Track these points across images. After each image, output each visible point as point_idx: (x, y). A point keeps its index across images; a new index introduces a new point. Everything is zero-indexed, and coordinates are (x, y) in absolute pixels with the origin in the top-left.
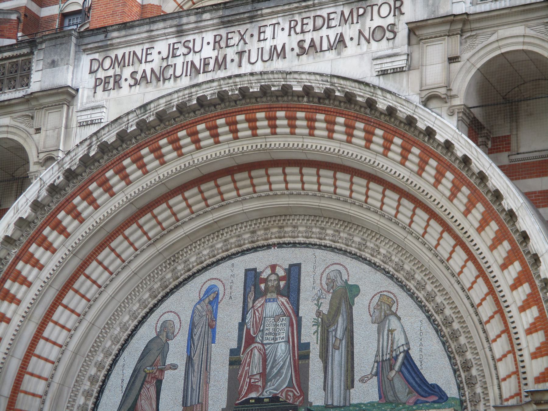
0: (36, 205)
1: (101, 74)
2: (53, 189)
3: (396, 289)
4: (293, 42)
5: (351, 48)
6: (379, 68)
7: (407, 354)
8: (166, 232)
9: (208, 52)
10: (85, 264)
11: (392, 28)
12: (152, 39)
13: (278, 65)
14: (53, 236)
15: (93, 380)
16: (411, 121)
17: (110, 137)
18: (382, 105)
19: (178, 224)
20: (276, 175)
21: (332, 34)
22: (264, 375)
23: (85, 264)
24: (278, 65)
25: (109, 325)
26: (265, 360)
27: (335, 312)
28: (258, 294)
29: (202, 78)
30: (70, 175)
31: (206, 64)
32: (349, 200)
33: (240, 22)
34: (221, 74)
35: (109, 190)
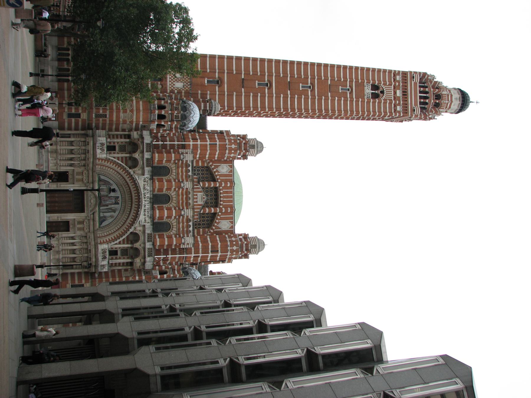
0: (128, 171)
1: (146, 179)
2: (130, 173)
3: (115, 218)
5: (144, 217)
6: (141, 221)
7: (106, 220)
8: (125, 186)
9: (147, 196)
10: (121, 175)
11: (146, 222)
13: (143, 206)
15: (105, 174)
16: (133, 226)
17: (136, 182)
18: (135, 221)
19: (126, 188)
20: (130, 203)
21: (146, 214)
22: (104, 200)
23: (121, 175)
25: (113, 176)
26: (107, 200)
29: (143, 195)
30: (132, 175)
31: (145, 196)
33: (150, 200)
34: (143, 198)
35: (130, 180)
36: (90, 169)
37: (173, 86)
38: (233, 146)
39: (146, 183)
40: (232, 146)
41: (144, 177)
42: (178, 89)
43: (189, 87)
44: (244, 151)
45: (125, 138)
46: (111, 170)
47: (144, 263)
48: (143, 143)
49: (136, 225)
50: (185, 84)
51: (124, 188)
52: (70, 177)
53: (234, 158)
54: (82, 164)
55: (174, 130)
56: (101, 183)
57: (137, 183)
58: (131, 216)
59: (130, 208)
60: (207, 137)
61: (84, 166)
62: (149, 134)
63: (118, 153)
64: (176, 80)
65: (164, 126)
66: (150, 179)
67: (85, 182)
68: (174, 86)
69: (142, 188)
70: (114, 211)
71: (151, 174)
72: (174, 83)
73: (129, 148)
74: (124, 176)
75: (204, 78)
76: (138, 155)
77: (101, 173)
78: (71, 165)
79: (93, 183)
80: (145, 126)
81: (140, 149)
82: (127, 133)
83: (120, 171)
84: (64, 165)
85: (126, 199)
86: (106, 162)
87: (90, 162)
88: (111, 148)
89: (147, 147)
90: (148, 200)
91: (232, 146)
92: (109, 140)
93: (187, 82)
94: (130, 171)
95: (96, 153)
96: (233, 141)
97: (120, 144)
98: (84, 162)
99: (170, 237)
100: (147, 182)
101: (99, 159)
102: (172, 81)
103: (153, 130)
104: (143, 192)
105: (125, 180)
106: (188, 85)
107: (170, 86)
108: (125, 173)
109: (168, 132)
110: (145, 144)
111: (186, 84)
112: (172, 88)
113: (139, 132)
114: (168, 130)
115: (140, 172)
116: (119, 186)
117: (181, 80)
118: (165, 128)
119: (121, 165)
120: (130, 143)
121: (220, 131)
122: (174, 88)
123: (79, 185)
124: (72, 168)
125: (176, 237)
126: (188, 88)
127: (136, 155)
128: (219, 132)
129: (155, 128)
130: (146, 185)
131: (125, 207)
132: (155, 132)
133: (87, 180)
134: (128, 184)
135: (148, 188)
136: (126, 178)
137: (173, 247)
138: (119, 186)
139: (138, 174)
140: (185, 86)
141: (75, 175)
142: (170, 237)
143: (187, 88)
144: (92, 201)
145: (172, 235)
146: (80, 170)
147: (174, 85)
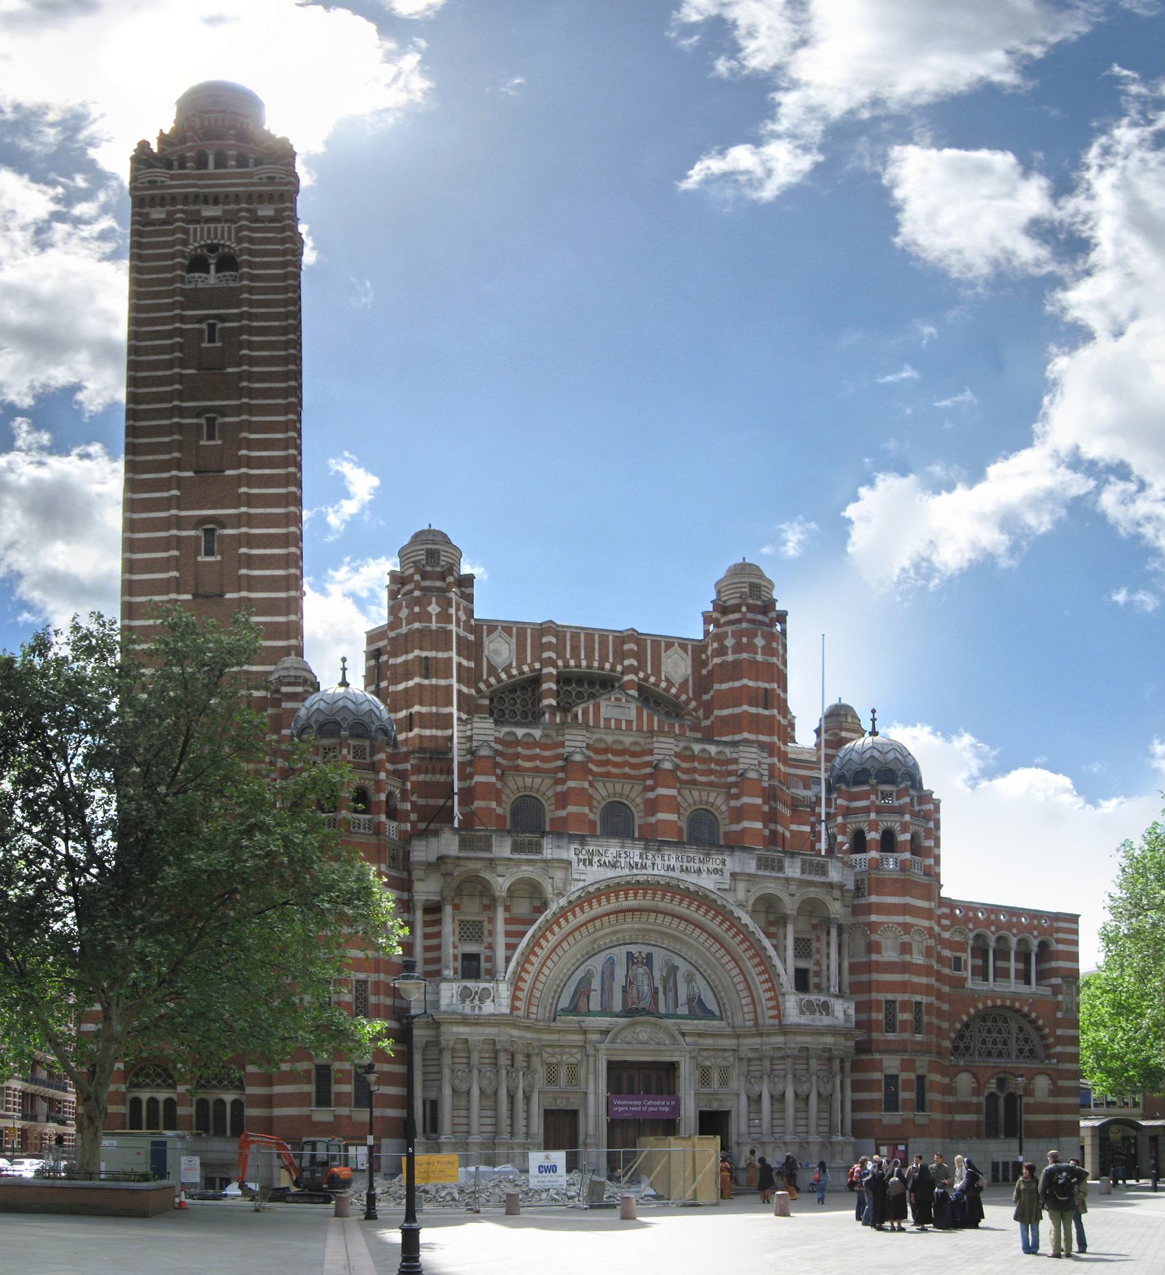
2: (563, 908)
4: (678, 865)
8: (596, 930)
9: (637, 859)
12: (608, 846)
13: (671, 874)
14: (556, 929)
17: (591, 889)
20: (653, 915)
22: (639, 999)
24: (671, 874)
27: (669, 975)
28: (634, 964)
29: (635, 871)
30: (570, 902)
32: (683, 932)
34: (644, 871)
36: (539, 1040)
38: (434, 609)
39: (596, 859)
40: (434, 613)
41: (575, 864)
44: (450, 579)
45: (438, 922)
46: (545, 970)
47: (841, 887)
48: (459, 858)
49: (729, 897)
51: (602, 933)
52: (561, 1104)
53: (470, 613)
54: (525, 1064)
55: (400, 767)
56: (583, 1008)
57: (596, 886)
58: (699, 916)
59: (668, 919)
60: (401, 687)
61: (528, 1056)
62: (424, 843)
63: (490, 947)
65: (390, 795)
66: (583, 844)
67: (578, 1056)
69: (610, 873)
70: (673, 970)
71: (564, 842)
73: (472, 909)
74: (567, 927)
76: (500, 880)
77: (551, 1004)
78: (527, 1098)
79: (585, 1032)
80: (393, 858)
81: (479, 871)
82: (419, 915)
83: (553, 940)
84: (524, 1122)
85: (638, 930)
86: (521, 984)
87: (520, 1037)
88: (471, 967)
89: (472, 848)
90: (650, 857)
91: (434, 613)
92: (448, 973)
94: (554, 907)
95: (493, 1015)
96: (417, 609)
97: (457, 938)
98: (520, 1059)
99: (738, 814)
100: (592, 854)
101: (513, 1008)
103: (402, 833)
104: (626, 871)
105: (578, 928)
108: (560, 927)
109: (409, 786)
110: (463, 854)
113: (417, 874)
114: (404, 784)
115: (559, 874)
116: (593, 949)
118: (397, 792)
119: (533, 936)
120: (456, 907)
121: (367, 659)
123: (591, 1077)
124: (535, 1096)
125: (737, 797)
127: (501, 884)
128: (373, 662)
129: (395, 824)
130: (603, 859)
131: (661, 933)
132: (408, 827)
133: (574, 1051)
134: (592, 920)
135: (612, 852)
136: (574, 922)
137: (766, 808)
138: (593, 949)
139: (566, 882)
141: (556, 1088)
142: (738, 814)
144: (644, 1036)
145: (731, 809)
146: (541, 1073)
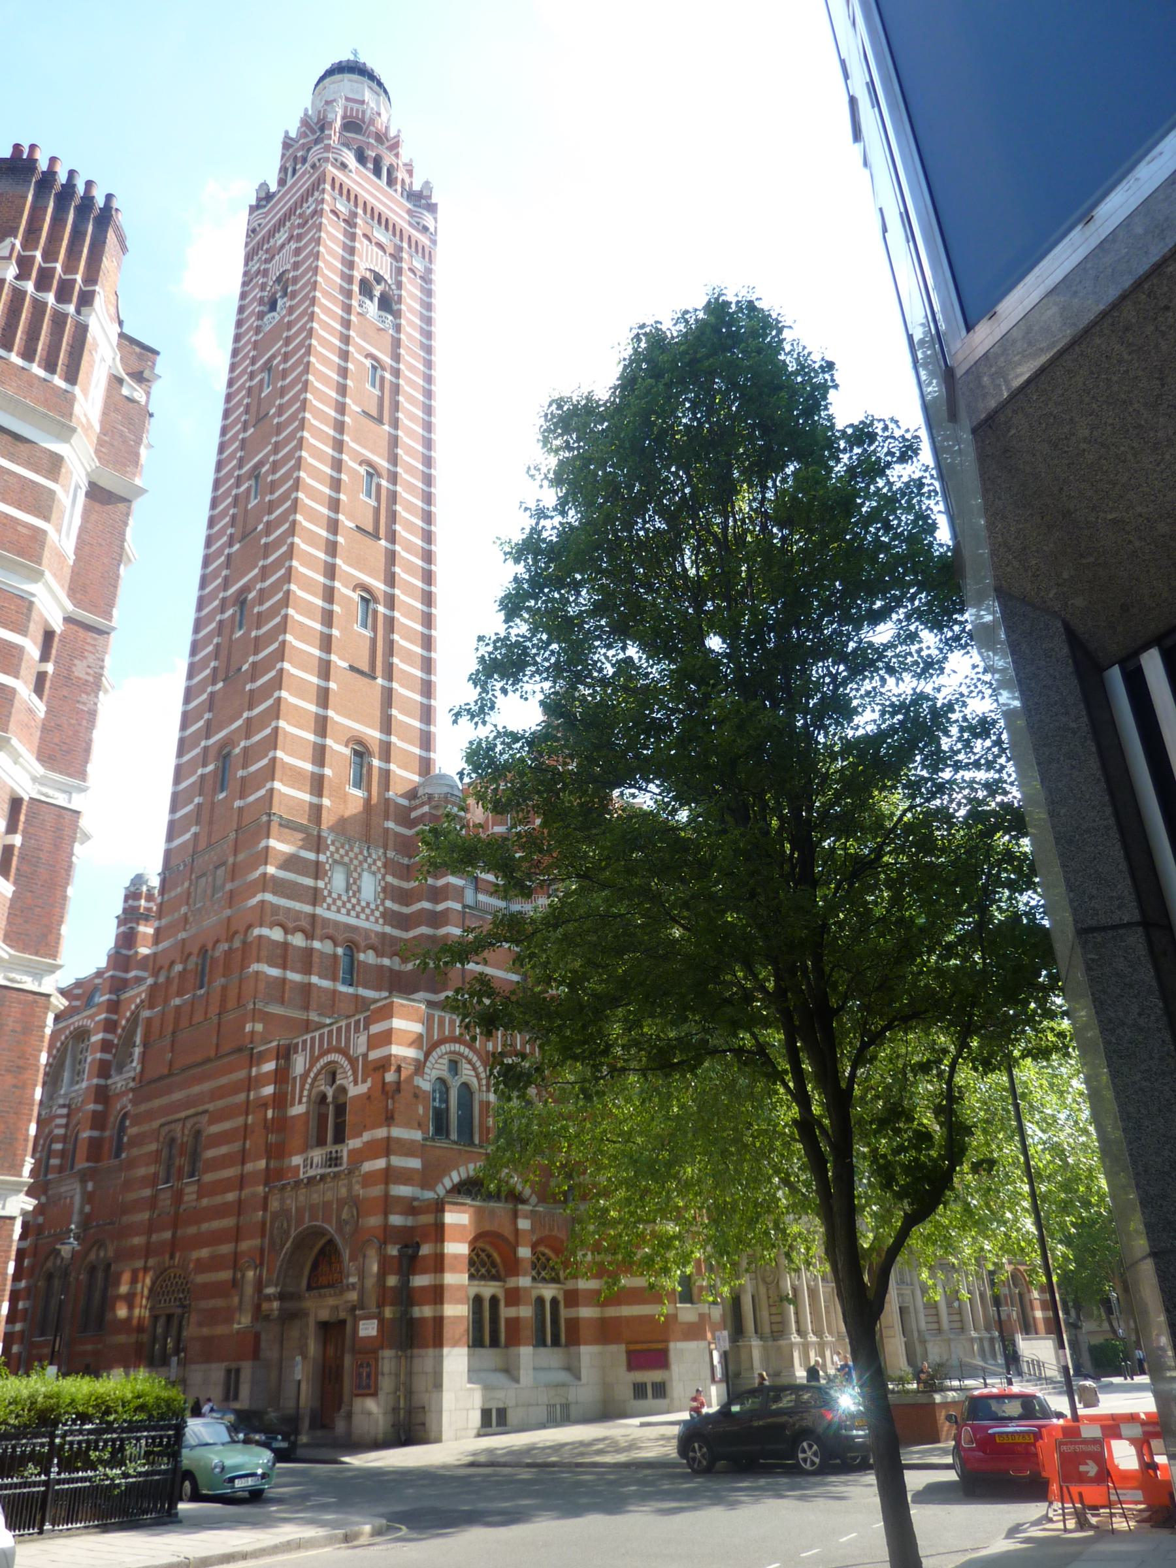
37: (372, 911)
42: (382, 895)
43: (374, 856)
50: (365, 866)
64: (354, 895)
68: (373, 906)
72: (363, 904)
75: (346, 794)
93: (360, 857)
102: (358, 909)
106: (370, 855)
107: (372, 919)
111: (366, 860)
112: (377, 914)
117: (355, 875)
122: (377, 909)
126: (379, 859)
140: (374, 868)
143: (379, 864)
147: (368, 904)
